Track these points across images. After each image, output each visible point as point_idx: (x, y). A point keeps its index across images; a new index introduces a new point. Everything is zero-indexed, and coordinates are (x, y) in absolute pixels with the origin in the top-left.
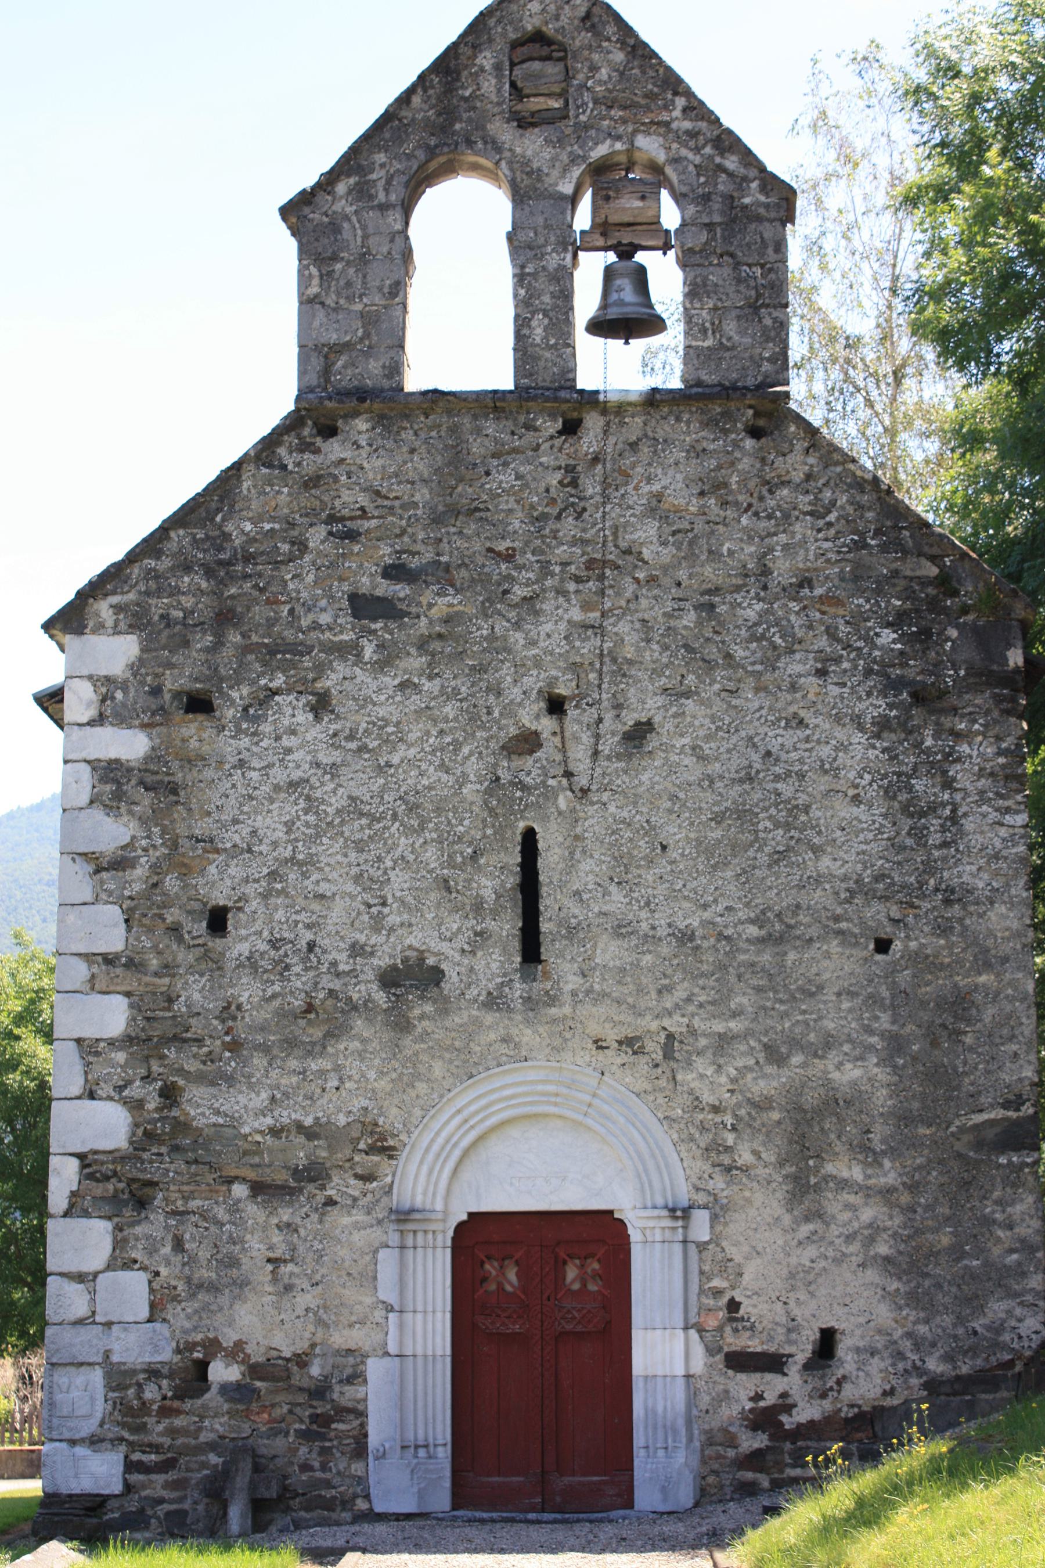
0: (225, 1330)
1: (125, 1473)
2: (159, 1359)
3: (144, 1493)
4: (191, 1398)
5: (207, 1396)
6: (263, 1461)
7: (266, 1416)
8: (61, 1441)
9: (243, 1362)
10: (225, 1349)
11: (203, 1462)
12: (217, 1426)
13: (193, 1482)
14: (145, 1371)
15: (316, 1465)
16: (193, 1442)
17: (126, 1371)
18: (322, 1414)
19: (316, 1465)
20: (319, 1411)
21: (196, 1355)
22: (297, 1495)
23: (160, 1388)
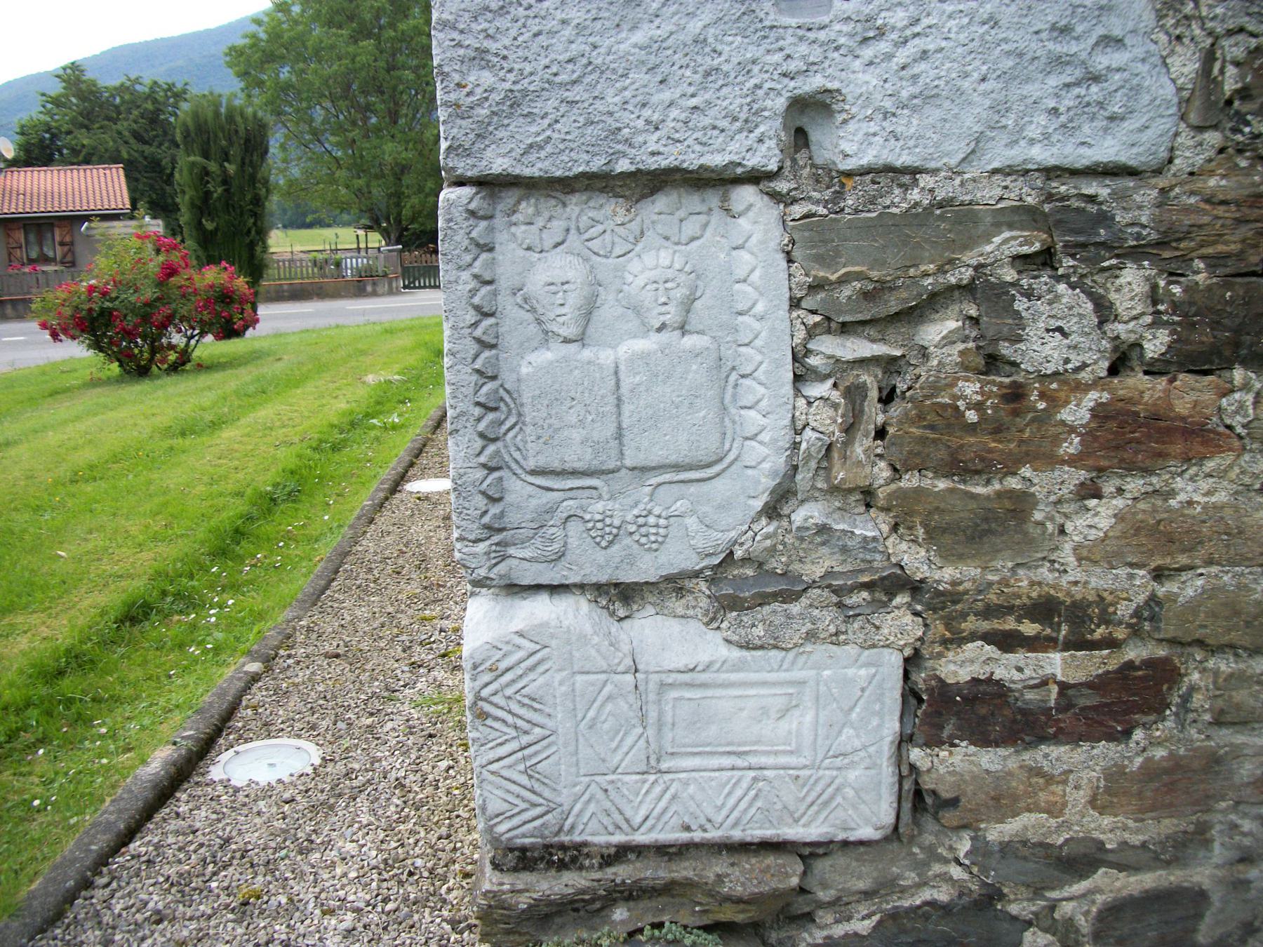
1: (905, 740)
2: (1108, 150)
3: (997, 832)
8: (555, 589)
14: (1025, 216)
17: (917, 217)
23: (1104, 311)
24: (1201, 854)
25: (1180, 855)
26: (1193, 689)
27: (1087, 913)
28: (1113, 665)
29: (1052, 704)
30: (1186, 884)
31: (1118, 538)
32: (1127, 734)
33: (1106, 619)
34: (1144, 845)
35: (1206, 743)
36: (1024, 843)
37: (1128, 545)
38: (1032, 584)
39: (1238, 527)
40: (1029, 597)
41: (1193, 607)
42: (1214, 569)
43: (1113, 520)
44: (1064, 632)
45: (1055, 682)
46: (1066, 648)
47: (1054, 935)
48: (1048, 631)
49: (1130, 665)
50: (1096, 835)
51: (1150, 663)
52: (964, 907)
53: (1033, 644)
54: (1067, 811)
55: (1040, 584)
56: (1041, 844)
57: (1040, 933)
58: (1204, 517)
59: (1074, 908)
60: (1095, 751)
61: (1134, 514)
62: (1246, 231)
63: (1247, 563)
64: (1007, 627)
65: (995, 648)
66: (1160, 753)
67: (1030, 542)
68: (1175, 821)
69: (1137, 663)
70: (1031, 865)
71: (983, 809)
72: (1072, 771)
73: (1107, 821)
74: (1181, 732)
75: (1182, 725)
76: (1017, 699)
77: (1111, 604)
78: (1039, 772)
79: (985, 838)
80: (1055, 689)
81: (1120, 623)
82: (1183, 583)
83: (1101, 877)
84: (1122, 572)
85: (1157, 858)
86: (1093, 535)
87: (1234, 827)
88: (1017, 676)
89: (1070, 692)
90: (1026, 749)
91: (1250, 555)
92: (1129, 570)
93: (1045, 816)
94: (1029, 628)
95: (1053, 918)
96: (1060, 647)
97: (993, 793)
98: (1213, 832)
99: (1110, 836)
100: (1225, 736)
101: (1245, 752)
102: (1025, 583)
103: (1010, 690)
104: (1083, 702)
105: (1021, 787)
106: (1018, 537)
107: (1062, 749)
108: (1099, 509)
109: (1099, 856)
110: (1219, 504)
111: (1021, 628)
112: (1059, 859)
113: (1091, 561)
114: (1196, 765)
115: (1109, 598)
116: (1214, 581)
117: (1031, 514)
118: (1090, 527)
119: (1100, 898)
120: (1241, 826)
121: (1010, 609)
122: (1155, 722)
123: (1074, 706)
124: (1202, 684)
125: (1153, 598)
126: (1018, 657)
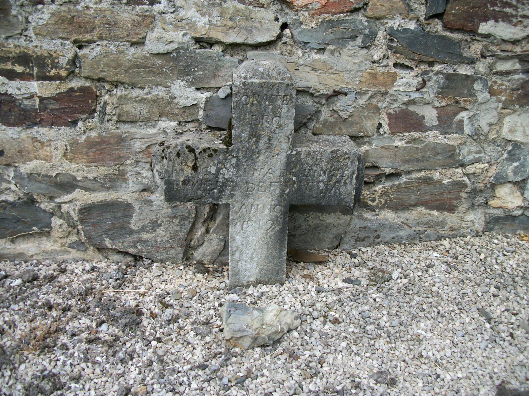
3: (26, 168)
11: (156, 101)
13: (138, 145)
16: (132, 53)
22: (378, 178)
24: (124, 185)
25: (113, 185)
26: (105, 103)
27: (74, 210)
28: (64, 88)
29: (37, 107)
30: (120, 200)
31: (53, 24)
32: (75, 123)
33: (55, 66)
34: (95, 179)
35: (117, 131)
36: (39, 174)
37: (59, 28)
38: (16, 46)
39: (114, 21)
40: (15, 53)
41: (96, 61)
42: (105, 42)
43: (50, 15)
44: (35, 72)
45: (37, 96)
46: (38, 80)
47: (64, 220)
48: (28, 70)
49: (72, 90)
50: (71, 173)
51: (82, 89)
52: (20, 204)
53: (22, 77)
54: (53, 160)
55: (19, 46)
56: (46, 176)
57: (58, 219)
58: (96, 15)
59: (68, 207)
60: (61, 131)
61: (60, 12)
63: (121, 40)
64: (9, 68)
65: (5, 78)
66: (94, 134)
67: (11, 25)
68: (106, 168)
69: (76, 89)
70: (43, 186)
71: (15, 157)
72: (52, 141)
73: (74, 166)
74: (101, 124)
75: (102, 121)
76: (20, 104)
77: (56, 58)
78: (35, 140)
79: (20, 171)
80: (37, 100)
81: (62, 68)
82: (92, 49)
83: (77, 193)
84: (58, 42)
85: (102, 186)
86: (41, 22)
88: (18, 92)
89: (45, 102)
90: (27, 128)
91: (122, 36)
92: (63, 41)
93: (44, 161)
94: (19, 69)
95: (61, 212)
96: (35, 79)
97: (18, 149)
98: (128, 175)
99: (77, 173)
100: (126, 128)
101: (136, 136)
102: (12, 46)
103: (16, 99)
104: (52, 107)
105: (30, 147)
106: (6, 23)
107: (45, 129)
108: (44, 10)
109: (74, 183)
110: (103, 9)
111: (15, 68)
112: (56, 183)
113: (42, 35)
114: (112, 141)
115: (55, 55)
116: (105, 48)
117: (10, 12)
118: (41, 19)
119: (79, 203)
120: (143, 174)
121: (8, 59)
122: (87, 119)
123: (47, 108)
124: (110, 101)
125: (76, 56)
126: (16, 83)
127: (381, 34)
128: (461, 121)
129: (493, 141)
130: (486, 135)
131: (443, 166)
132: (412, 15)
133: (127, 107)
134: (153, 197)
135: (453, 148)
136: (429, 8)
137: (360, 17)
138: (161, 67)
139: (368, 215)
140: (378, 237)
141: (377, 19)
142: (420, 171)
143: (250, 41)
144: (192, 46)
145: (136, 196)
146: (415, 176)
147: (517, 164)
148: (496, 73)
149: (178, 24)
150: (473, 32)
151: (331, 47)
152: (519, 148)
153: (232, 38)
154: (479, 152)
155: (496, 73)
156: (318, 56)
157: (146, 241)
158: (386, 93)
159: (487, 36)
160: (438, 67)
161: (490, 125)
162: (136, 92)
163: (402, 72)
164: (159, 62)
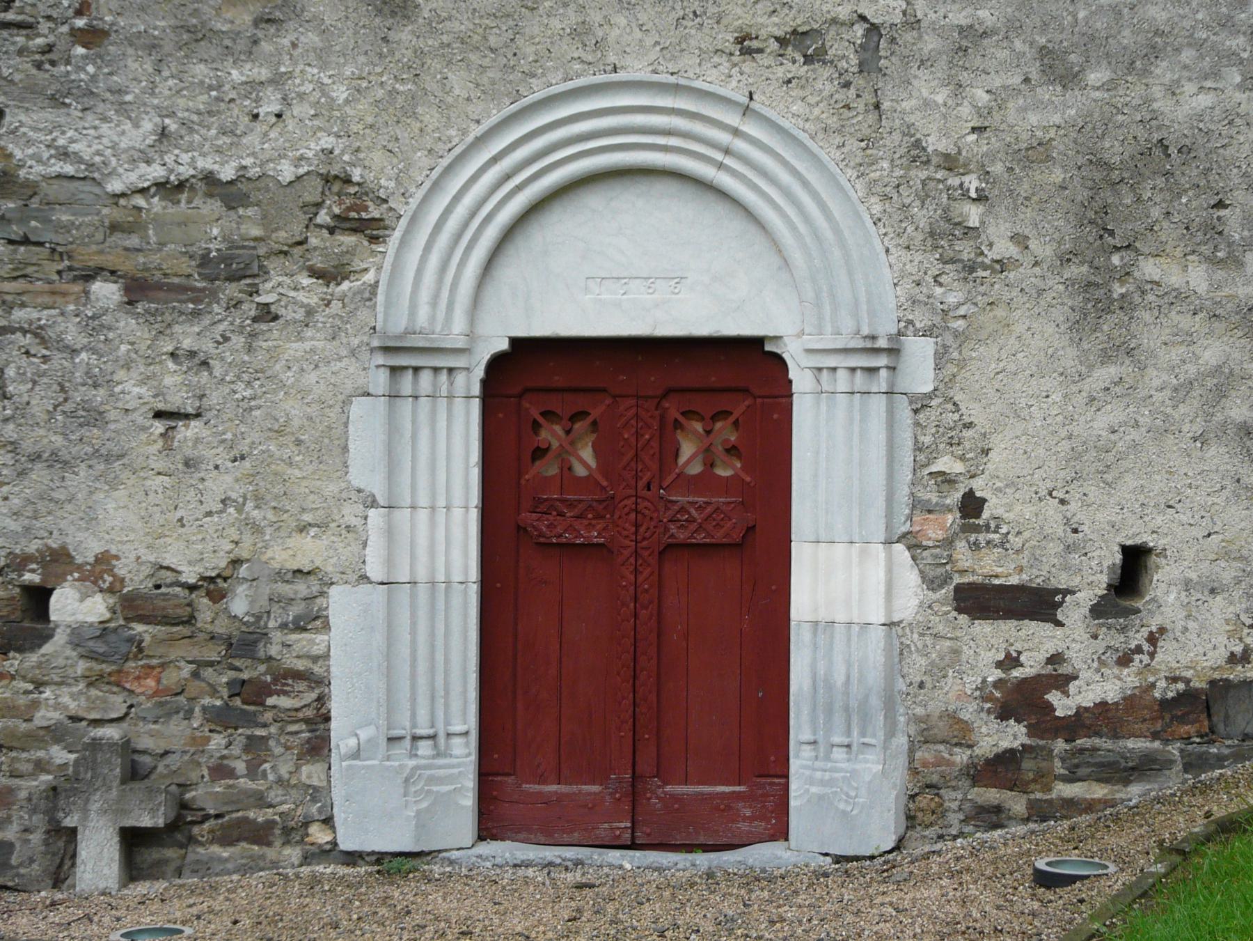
0: (81, 536)
4: (20, 650)
5: (47, 648)
6: (146, 759)
7: (151, 683)
9: (111, 590)
10: (79, 568)
12: (66, 700)
13: (23, 794)
15: (240, 767)
16: (24, 726)
18: (250, 680)
19: (240, 767)
20: (245, 676)
21: (28, 577)
22: (206, 818)
42: (5, 720)
62: (9, 608)
87: (21, 817)
100: (17, 781)
127: (197, 709)
128: (265, 771)
129: (295, 785)
130: (288, 781)
131: (255, 807)
132: (217, 695)
133: (17, 765)
134: (31, 837)
135: (261, 792)
136: (229, 689)
137: (181, 699)
138: (44, 736)
139: (201, 850)
140: (209, 869)
141: (193, 699)
142: (238, 811)
143: (107, 717)
144: (67, 722)
145: (18, 835)
146: (235, 815)
147: (319, 804)
148: (288, 733)
149: (57, 706)
150: (262, 704)
151: (162, 720)
152: (318, 791)
153: (94, 715)
154: (285, 795)
155: (288, 733)
156: (153, 726)
157: (23, 875)
158: (203, 751)
159: (274, 707)
160: (240, 731)
161: (291, 773)
162: (24, 755)
163: (215, 735)
164: (42, 733)
